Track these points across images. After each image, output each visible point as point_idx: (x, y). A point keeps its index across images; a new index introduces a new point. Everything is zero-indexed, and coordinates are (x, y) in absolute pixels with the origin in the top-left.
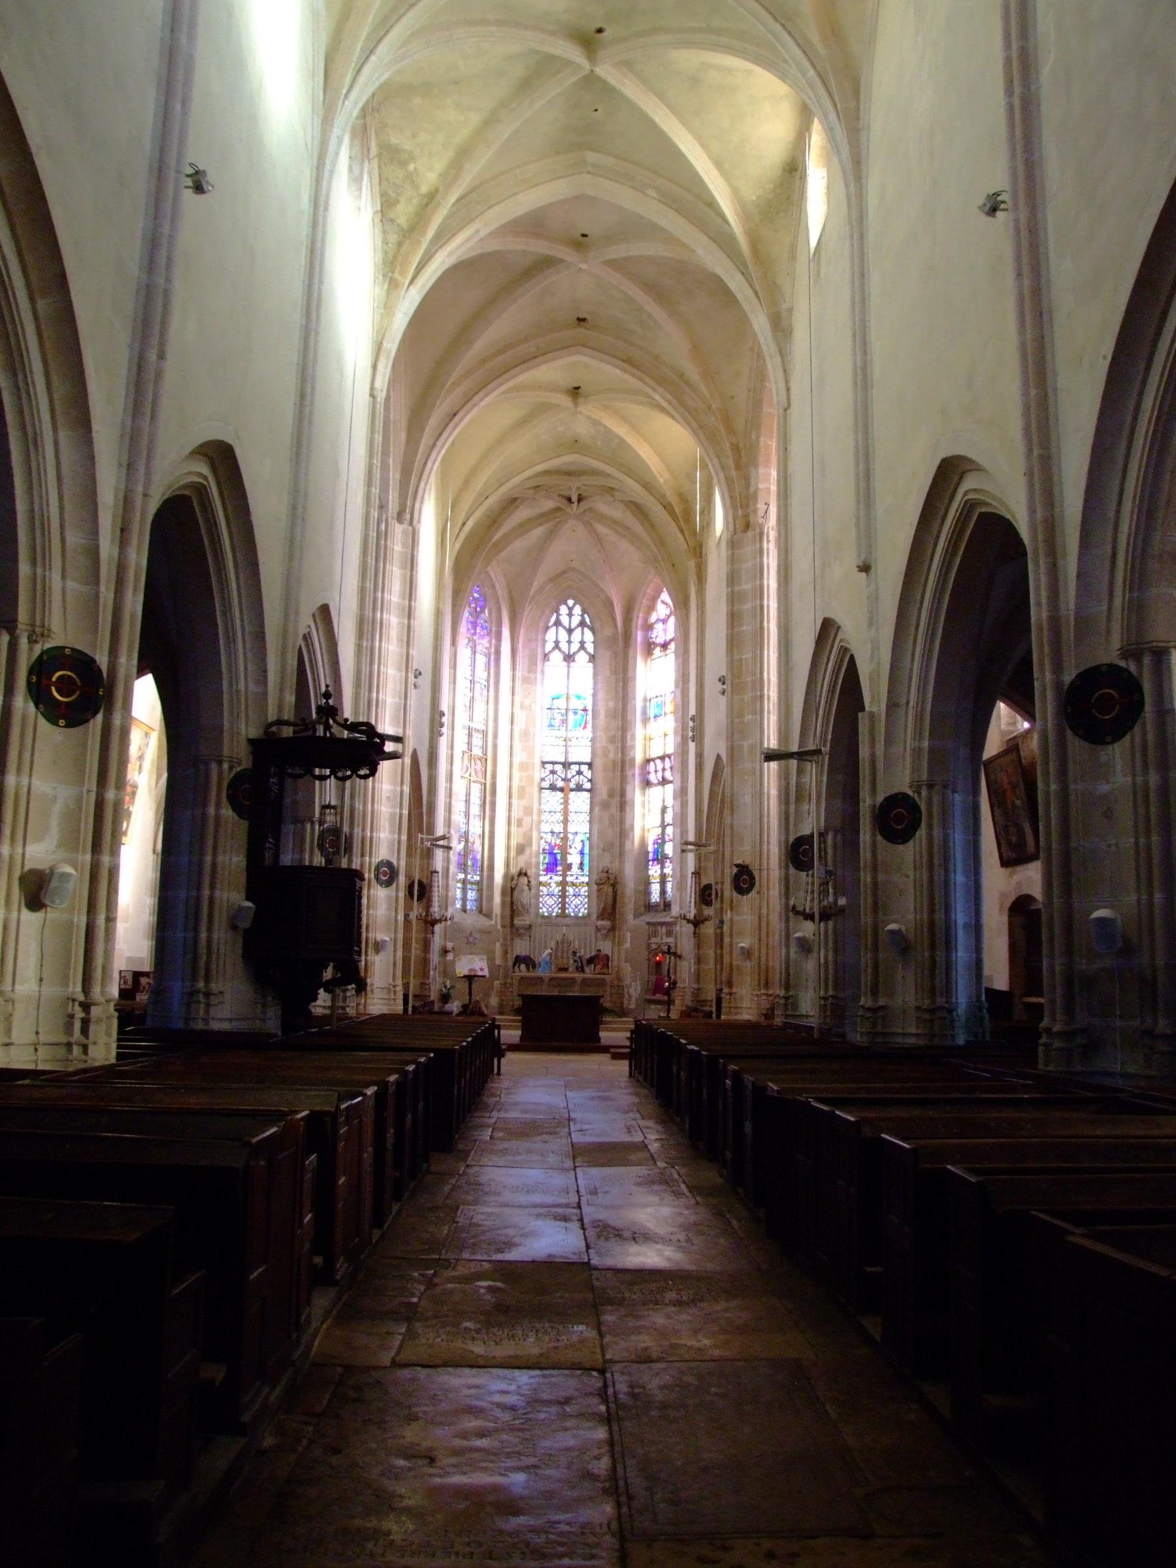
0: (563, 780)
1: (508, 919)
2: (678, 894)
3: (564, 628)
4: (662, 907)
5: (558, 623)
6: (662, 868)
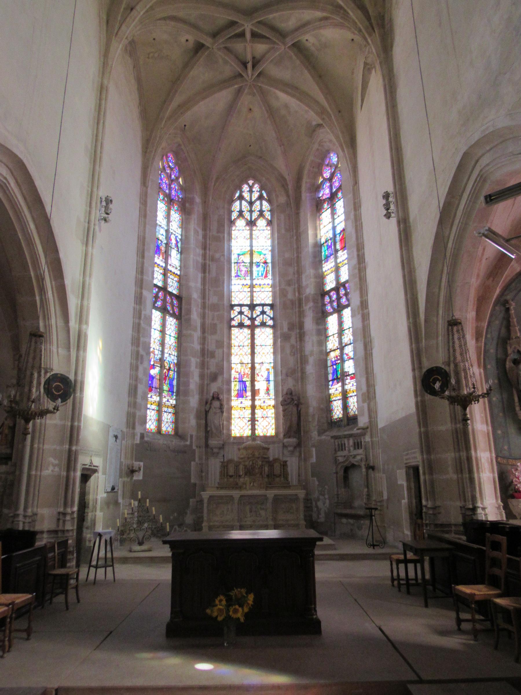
0: (249, 319)
1: (203, 440)
2: (366, 405)
3: (246, 201)
4: (345, 422)
5: (241, 198)
6: (343, 385)
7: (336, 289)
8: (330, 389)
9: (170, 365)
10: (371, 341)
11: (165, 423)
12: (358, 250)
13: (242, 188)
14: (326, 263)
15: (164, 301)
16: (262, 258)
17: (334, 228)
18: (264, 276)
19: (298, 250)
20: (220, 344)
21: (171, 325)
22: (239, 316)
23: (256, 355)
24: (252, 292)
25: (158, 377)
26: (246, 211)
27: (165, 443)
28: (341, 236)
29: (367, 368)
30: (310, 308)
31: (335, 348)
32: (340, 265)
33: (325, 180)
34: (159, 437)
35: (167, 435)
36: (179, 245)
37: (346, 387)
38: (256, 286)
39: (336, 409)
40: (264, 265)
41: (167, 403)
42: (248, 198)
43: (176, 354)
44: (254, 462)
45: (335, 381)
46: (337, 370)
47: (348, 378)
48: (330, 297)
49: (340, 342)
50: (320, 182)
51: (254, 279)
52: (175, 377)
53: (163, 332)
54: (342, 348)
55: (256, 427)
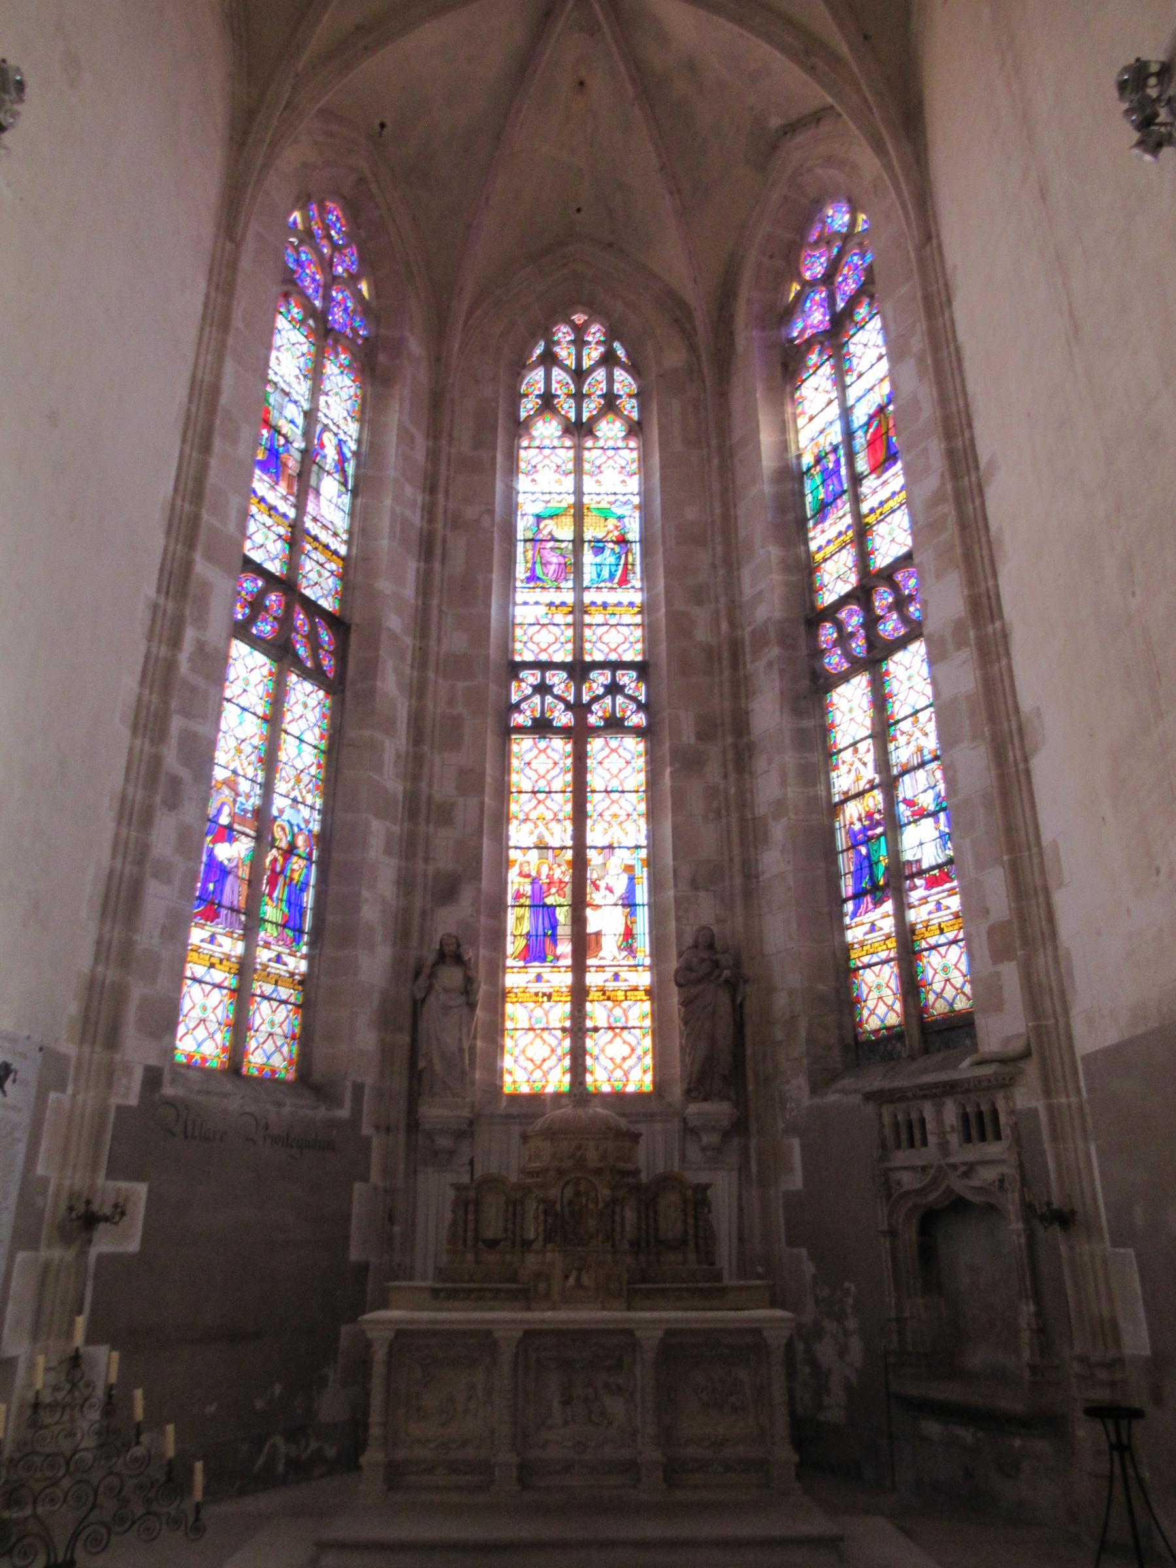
0: (569, 707)
3: (565, 368)
5: (549, 359)
6: (901, 908)
7: (862, 595)
8: (849, 927)
9: (294, 836)
10: (1020, 730)
11: (261, 1037)
12: (949, 434)
13: (554, 334)
14: (820, 526)
15: (285, 622)
16: (611, 527)
17: (846, 413)
18: (616, 580)
19: (728, 496)
20: (471, 781)
21: (305, 705)
22: (537, 699)
23: (589, 822)
24: (578, 627)
25: (244, 873)
26: (563, 397)
27: (253, 1108)
28: (871, 430)
29: (1009, 829)
30: (770, 664)
31: (862, 785)
32: (871, 519)
33: (813, 284)
34: (228, 1086)
35: (267, 1082)
36: (350, 468)
37: (912, 916)
38: (593, 608)
39: (874, 995)
40: (617, 549)
41: (276, 967)
42: (571, 362)
43: (319, 803)
44: (582, 1188)
45: (868, 898)
46: (874, 859)
47: (919, 882)
48: (839, 626)
49: (883, 762)
50: (792, 295)
51: (588, 588)
52: (312, 881)
53: (273, 720)
54: (889, 782)
55: (589, 1061)
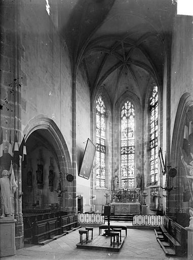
5: (124, 109)
15: (100, 148)
53: (100, 157)
